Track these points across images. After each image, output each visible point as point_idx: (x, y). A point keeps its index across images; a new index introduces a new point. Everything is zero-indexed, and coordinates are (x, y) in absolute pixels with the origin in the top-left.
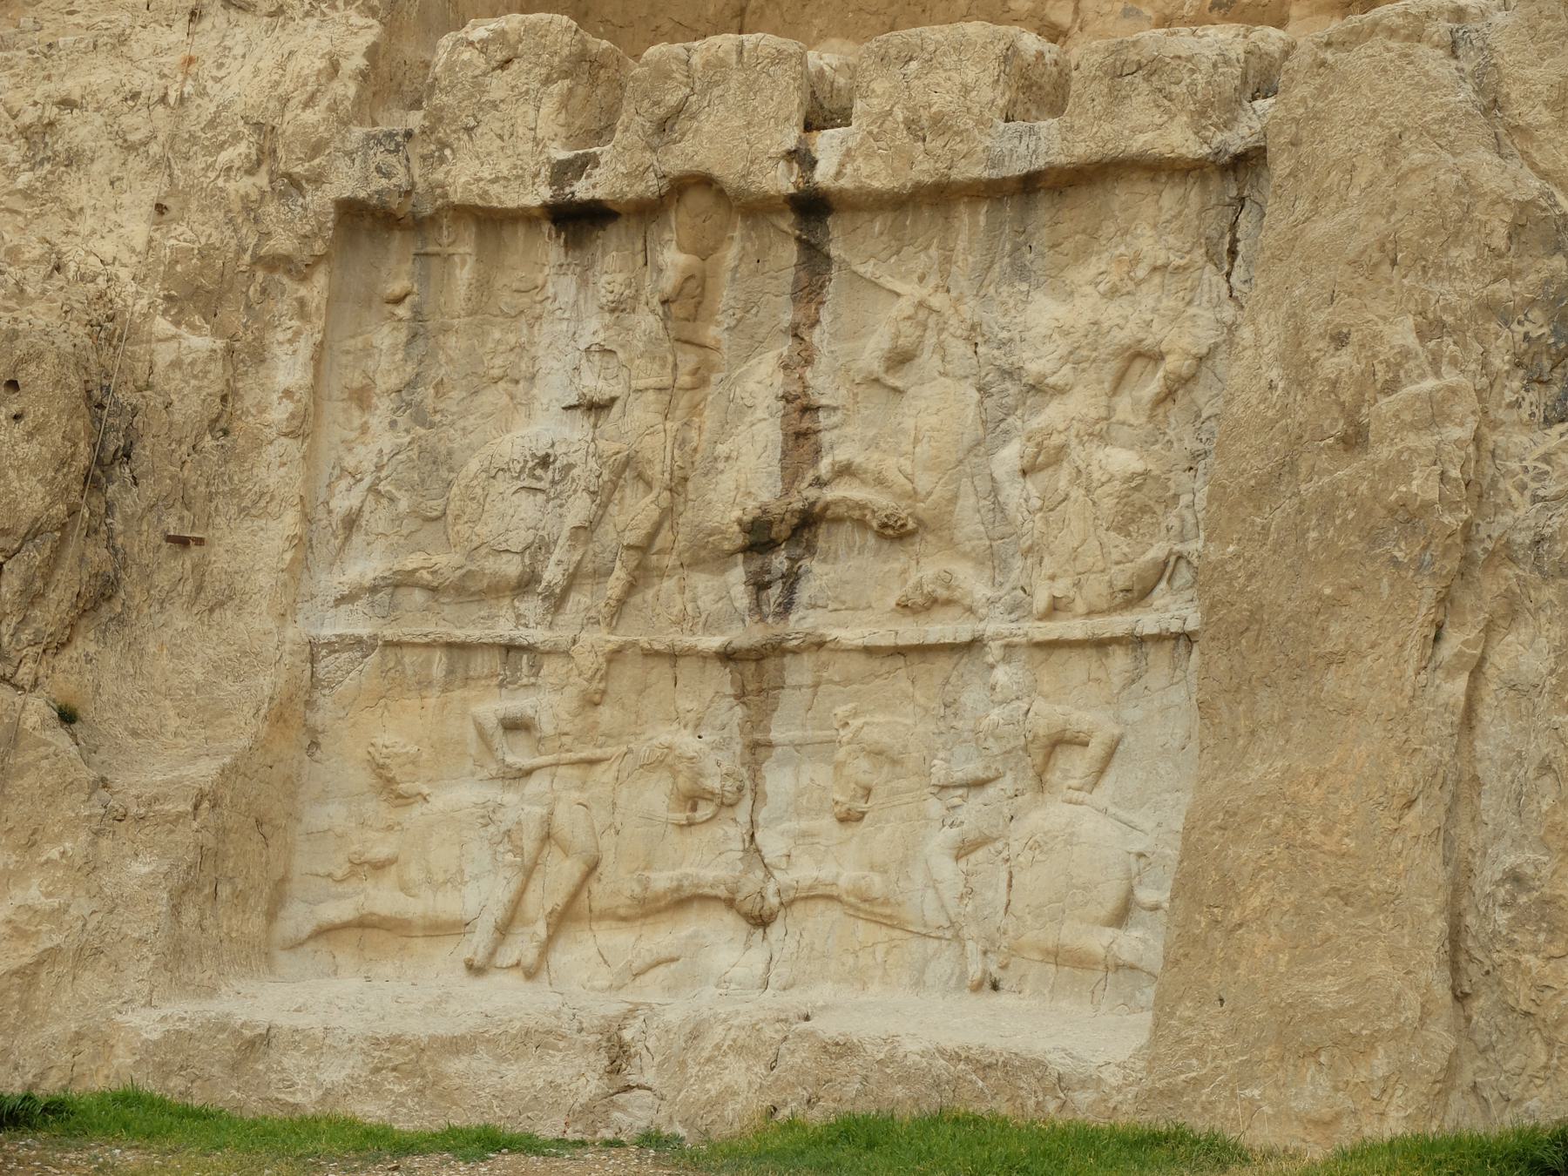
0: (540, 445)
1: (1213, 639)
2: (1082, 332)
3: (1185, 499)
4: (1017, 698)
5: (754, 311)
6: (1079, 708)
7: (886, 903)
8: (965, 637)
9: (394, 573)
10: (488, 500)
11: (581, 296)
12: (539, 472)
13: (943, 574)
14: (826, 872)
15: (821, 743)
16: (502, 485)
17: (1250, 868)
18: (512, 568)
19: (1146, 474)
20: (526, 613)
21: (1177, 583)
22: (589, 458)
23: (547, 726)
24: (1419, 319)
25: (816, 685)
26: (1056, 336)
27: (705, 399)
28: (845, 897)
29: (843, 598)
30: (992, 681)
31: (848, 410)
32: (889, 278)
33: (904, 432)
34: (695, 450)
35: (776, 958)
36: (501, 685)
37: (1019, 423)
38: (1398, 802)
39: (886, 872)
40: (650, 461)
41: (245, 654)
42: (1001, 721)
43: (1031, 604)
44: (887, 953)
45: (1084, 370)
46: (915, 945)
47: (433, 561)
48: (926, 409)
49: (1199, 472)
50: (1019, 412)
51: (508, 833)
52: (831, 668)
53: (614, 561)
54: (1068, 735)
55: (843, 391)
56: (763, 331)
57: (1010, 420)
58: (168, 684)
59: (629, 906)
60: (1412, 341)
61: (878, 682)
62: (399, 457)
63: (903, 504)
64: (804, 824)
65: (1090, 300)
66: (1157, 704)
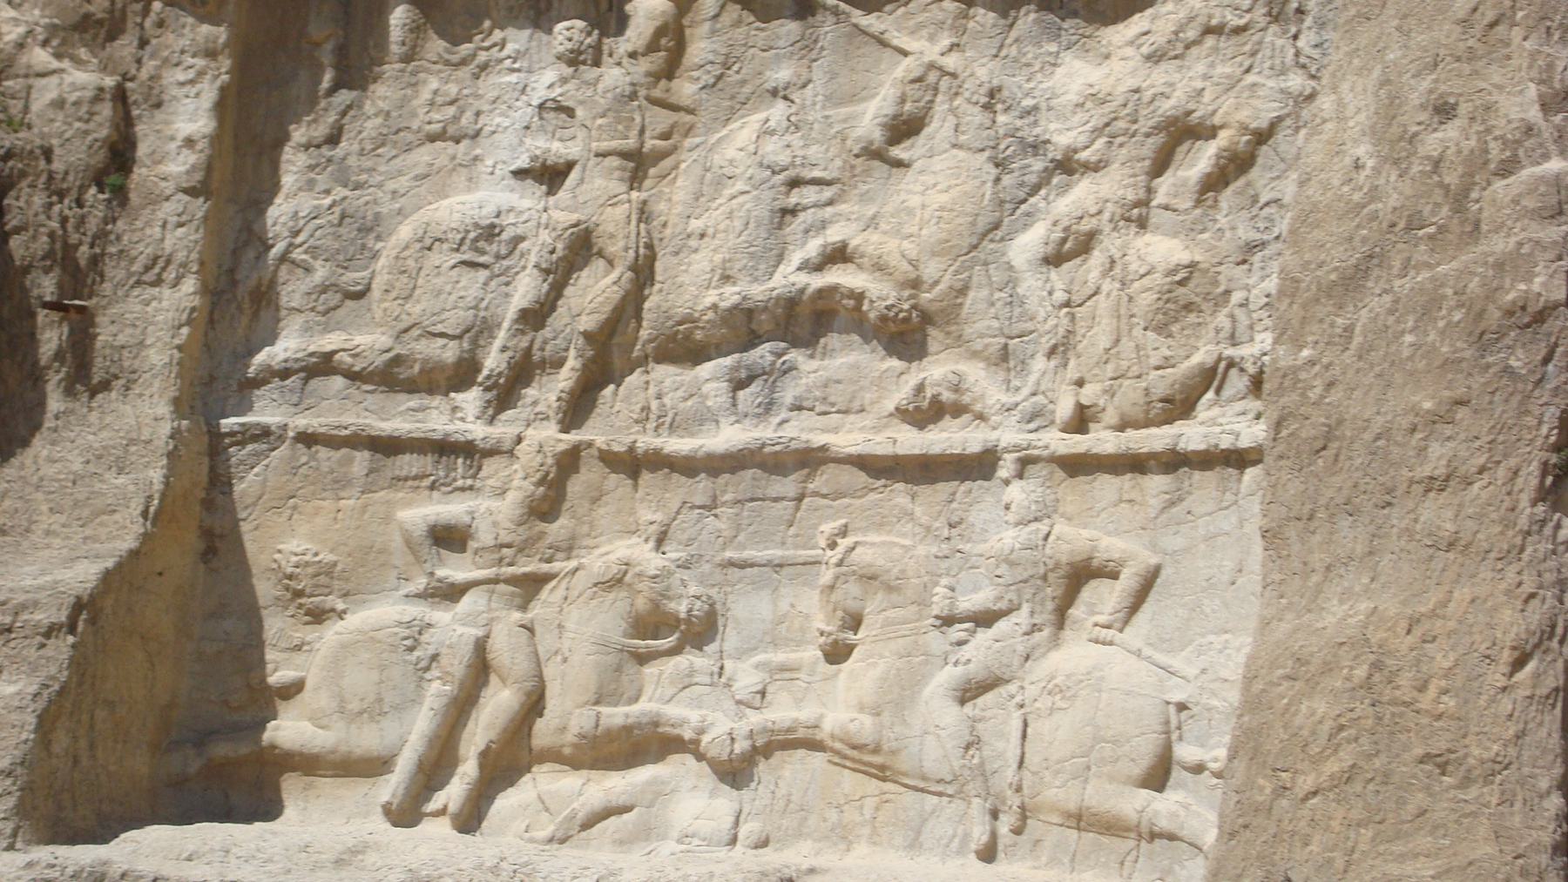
0: (484, 212)
1: (1281, 457)
2: (1121, 100)
3: (1237, 297)
4: (1036, 519)
5: (735, 68)
6: (1109, 534)
7: (876, 750)
8: (974, 448)
9: (312, 355)
10: (422, 274)
11: (534, 44)
12: (481, 244)
13: (951, 377)
14: (805, 714)
15: (804, 564)
16: (435, 258)
17: (1327, 727)
18: (449, 353)
19: (1192, 266)
20: (464, 405)
21: (1227, 392)
22: (541, 230)
23: (484, 536)
24: (1543, 89)
25: (800, 499)
26: (1089, 105)
27: (676, 167)
28: (829, 743)
29: (832, 399)
30: (1006, 499)
31: (844, 184)
32: (896, 34)
33: (910, 212)
34: (665, 225)
35: (745, 811)
36: (432, 487)
37: (1042, 204)
38: (1507, 656)
39: (878, 714)
40: (612, 236)
41: (132, 442)
42: (1018, 546)
43: (1053, 412)
44: (877, 809)
45: (1121, 145)
46: (910, 796)
47: (356, 343)
48: (935, 185)
49: (1257, 265)
50: (1043, 192)
51: (435, 657)
52: (817, 478)
53: (567, 350)
54: (1095, 563)
55: (838, 163)
56: (747, 89)
57: (1032, 200)
58: (41, 473)
59: (575, 746)
60: (1534, 114)
61: (873, 496)
62: (317, 221)
63: (906, 293)
64: (780, 657)
65: (1131, 63)
66: (1202, 531)
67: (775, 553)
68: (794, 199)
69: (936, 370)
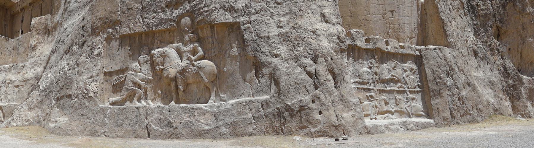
18: (366, 81)
67: (393, 97)
68: (389, 71)
69: (399, 84)
